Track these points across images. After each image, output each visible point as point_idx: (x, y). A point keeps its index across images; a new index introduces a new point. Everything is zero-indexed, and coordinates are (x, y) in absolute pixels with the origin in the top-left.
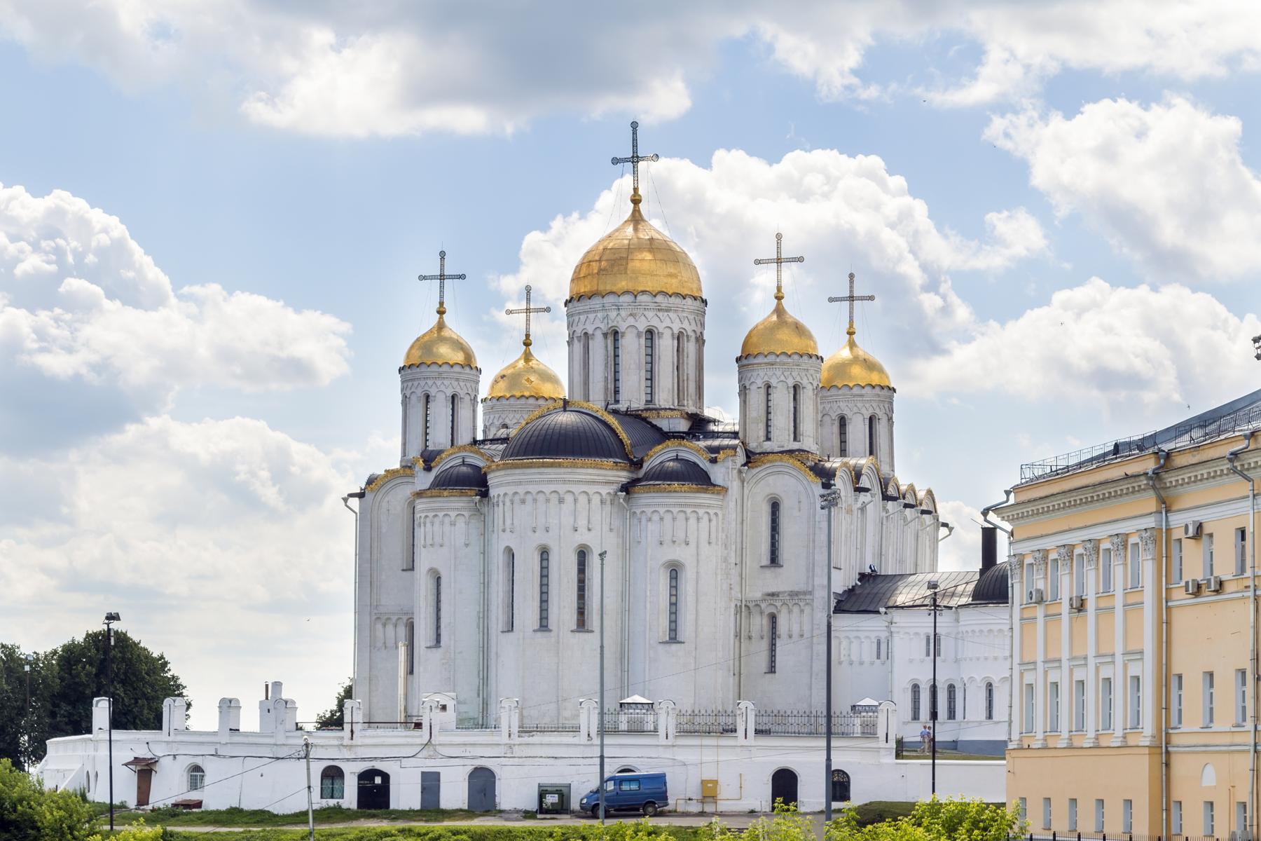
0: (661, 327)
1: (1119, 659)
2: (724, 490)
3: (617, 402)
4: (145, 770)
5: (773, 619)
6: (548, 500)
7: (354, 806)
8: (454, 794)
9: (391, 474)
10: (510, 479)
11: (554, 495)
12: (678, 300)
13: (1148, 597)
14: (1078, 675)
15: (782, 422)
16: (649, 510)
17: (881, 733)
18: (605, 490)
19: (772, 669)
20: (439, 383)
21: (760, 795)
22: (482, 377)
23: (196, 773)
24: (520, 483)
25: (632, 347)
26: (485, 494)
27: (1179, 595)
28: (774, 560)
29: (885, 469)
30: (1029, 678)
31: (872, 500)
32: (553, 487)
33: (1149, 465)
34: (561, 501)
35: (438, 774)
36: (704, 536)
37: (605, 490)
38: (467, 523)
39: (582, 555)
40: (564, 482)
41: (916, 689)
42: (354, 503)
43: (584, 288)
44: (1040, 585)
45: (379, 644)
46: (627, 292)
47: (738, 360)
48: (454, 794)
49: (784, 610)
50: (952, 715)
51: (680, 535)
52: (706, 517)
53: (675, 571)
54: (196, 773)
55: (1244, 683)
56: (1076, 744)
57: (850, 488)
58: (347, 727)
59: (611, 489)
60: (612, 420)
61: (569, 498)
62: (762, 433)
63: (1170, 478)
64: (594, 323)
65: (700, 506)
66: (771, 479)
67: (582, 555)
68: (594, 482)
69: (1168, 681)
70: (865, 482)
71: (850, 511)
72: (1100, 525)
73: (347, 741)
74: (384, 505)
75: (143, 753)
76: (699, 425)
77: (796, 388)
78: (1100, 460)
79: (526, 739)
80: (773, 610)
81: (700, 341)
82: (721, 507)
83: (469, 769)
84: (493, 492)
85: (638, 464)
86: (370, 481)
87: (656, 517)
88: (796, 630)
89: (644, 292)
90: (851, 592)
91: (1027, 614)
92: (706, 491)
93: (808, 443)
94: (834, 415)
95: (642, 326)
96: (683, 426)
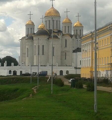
2: (59, 39)
5: (66, 53)
7: (13, 75)
18: (47, 38)
19: (66, 59)
22: (35, 26)
24: (36, 38)
26: (33, 39)
28: (66, 46)
34: (41, 40)
35: (22, 71)
39: (43, 46)
42: (20, 40)
44: (83, 49)
49: (67, 52)
58: (12, 66)
62: (65, 32)
63: (93, 36)
67: (43, 46)
68: (44, 38)
76: (59, 31)
81: (60, 21)
84: (34, 39)
88: (68, 55)
90: (75, 50)
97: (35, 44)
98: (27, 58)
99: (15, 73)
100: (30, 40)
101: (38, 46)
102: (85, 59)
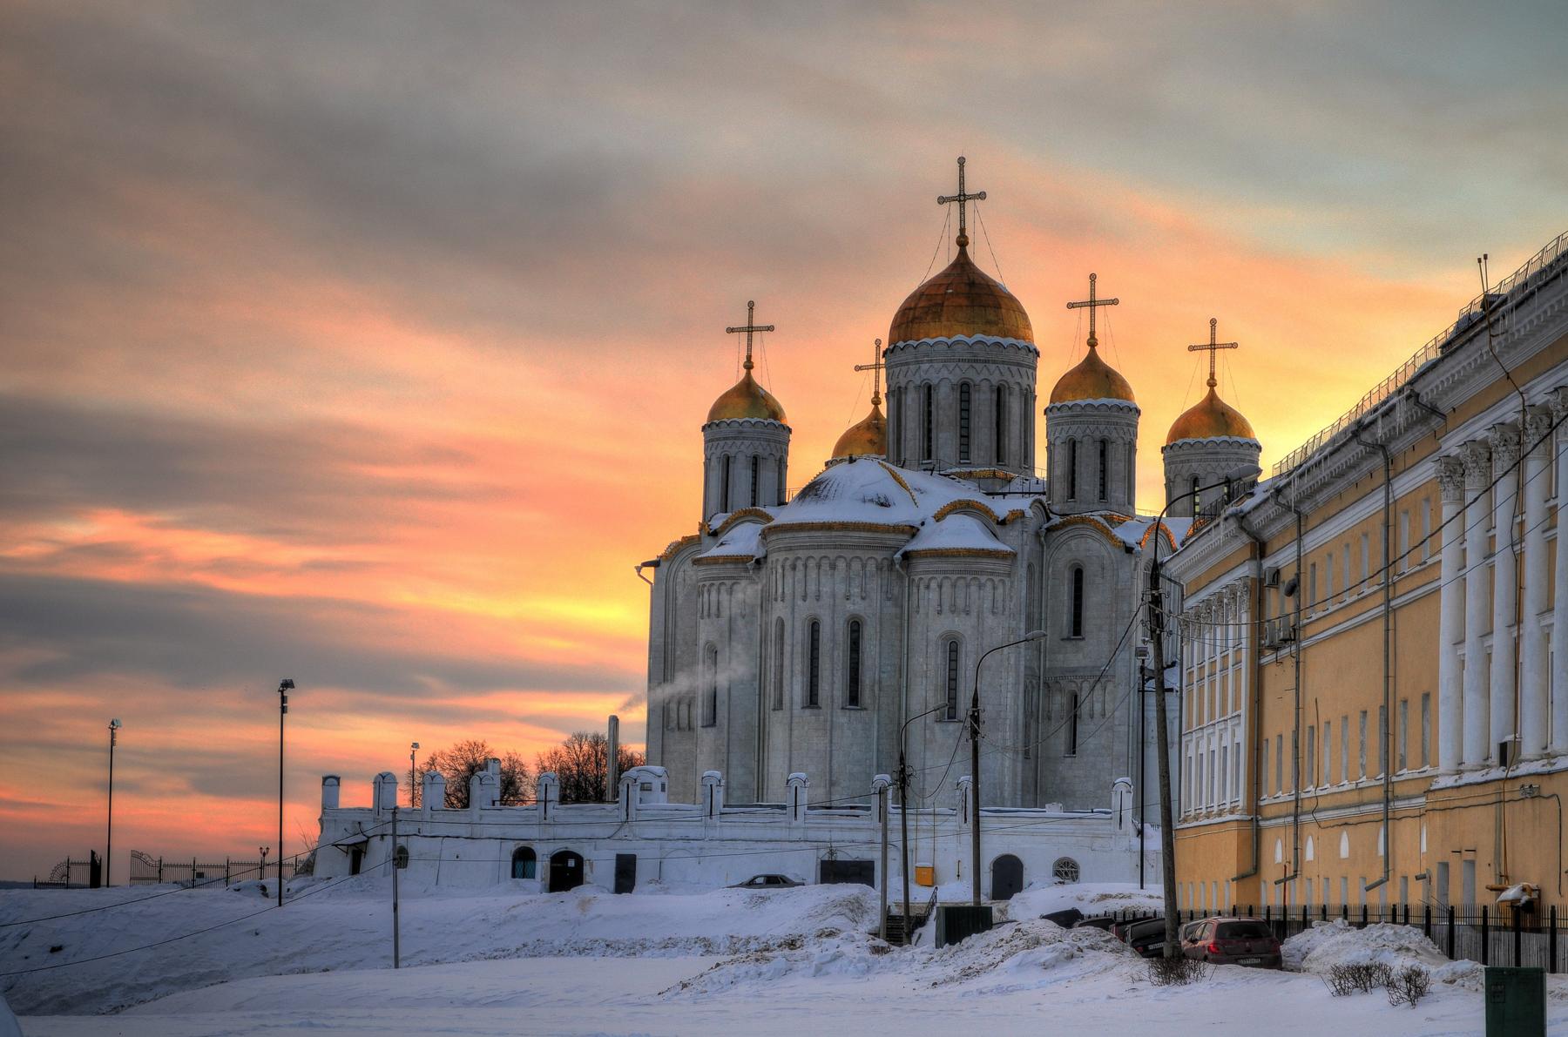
0: (977, 379)
6: (819, 566)
11: (825, 561)
20: (738, 442)
32: (823, 553)
34: (833, 567)
36: (987, 604)
37: (879, 555)
39: (855, 628)
42: (649, 573)
45: (673, 724)
51: (960, 603)
52: (989, 584)
61: (841, 565)
65: (982, 572)
66: (1073, 543)
67: (855, 628)
74: (681, 574)
77: (1104, 442)
80: (1073, 687)
82: (1009, 575)
87: (934, 585)
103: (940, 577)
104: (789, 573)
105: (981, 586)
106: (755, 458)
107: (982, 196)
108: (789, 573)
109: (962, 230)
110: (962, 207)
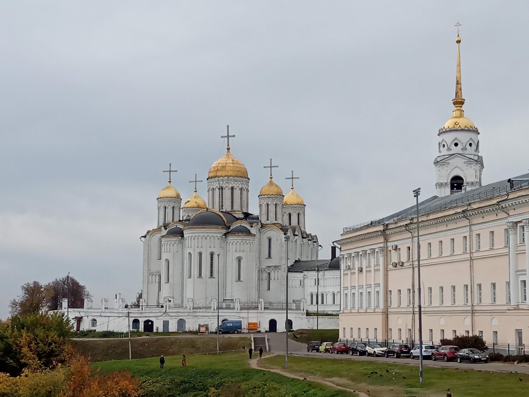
0: (236, 186)
1: (373, 286)
2: (255, 235)
3: (223, 209)
4: (79, 320)
5: (269, 274)
8: (173, 327)
9: (154, 230)
10: (190, 232)
12: (241, 178)
13: (381, 267)
14: (361, 291)
15: (272, 215)
16: (232, 241)
17: (302, 309)
19: (269, 289)
21: (265, 326)
23: (94, 322)
24: (193, 233)
25: (227, 193)
26: (183, 236)
27: (390, 267)
29: (303, 229)
30: (346, 292)
31: (299, 238)
32: (203, 234)
33: (381, 228)
34: (206, 238)
37: (219, 235)
38: (177, 245)
39: (212, 255)
40: (207, 233)
41: (312, 294)
42: (143, 239)
43: (211, 175)
44: (349, 264)
45: (150, 282)
46: (225, 176)
47: (259, 196)
48: (173, 327)
50: (323, 303)
53: (239, 260)
54: (94, 322)
55: (410, 293)
56: (360, 311)
57: (292, 235)
58: (141, 307)
59: (221, 235)
60: (221, 214)
61: (208, 238)
62: (266, 218)
63: (388, 232)
64: (216, 185)
67: (212, 255)
69: (387, 293)
70: (296, 233)
71: (292, 242)
72: (367, 246)
73: (141, 311)
75: (78, 315)
76: (247, 215)
78: (367, 226)
79: (195, 310)
81: (248, 190)
82: (254, 240)
83: (177, 320)
84: (185, 236)
85: (230, 227)
86: (148, 232)
89: (230, 176)
91: (346, 272)
92: (249, 236)
93: (280, 221)
94: (287, 213)
95: (230, 186)
96: (242, 216)
97: (187, 251)
98: (165, 287)
99: (149, 326)
100: (174, 239)
101: (199, 256)
102: (356, 291)
103: (236, 241)
104: (193, 240)
105: (247, 244)
106: (173, 207)
107: (234, 136)
108: (193, 240)
109: (228, 145)
110: (228, 139)
